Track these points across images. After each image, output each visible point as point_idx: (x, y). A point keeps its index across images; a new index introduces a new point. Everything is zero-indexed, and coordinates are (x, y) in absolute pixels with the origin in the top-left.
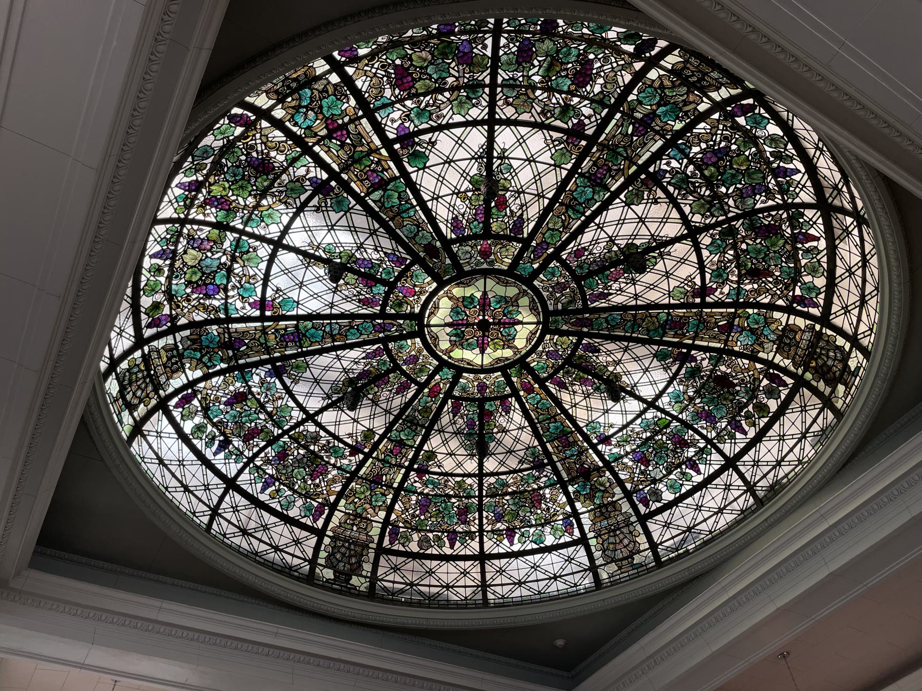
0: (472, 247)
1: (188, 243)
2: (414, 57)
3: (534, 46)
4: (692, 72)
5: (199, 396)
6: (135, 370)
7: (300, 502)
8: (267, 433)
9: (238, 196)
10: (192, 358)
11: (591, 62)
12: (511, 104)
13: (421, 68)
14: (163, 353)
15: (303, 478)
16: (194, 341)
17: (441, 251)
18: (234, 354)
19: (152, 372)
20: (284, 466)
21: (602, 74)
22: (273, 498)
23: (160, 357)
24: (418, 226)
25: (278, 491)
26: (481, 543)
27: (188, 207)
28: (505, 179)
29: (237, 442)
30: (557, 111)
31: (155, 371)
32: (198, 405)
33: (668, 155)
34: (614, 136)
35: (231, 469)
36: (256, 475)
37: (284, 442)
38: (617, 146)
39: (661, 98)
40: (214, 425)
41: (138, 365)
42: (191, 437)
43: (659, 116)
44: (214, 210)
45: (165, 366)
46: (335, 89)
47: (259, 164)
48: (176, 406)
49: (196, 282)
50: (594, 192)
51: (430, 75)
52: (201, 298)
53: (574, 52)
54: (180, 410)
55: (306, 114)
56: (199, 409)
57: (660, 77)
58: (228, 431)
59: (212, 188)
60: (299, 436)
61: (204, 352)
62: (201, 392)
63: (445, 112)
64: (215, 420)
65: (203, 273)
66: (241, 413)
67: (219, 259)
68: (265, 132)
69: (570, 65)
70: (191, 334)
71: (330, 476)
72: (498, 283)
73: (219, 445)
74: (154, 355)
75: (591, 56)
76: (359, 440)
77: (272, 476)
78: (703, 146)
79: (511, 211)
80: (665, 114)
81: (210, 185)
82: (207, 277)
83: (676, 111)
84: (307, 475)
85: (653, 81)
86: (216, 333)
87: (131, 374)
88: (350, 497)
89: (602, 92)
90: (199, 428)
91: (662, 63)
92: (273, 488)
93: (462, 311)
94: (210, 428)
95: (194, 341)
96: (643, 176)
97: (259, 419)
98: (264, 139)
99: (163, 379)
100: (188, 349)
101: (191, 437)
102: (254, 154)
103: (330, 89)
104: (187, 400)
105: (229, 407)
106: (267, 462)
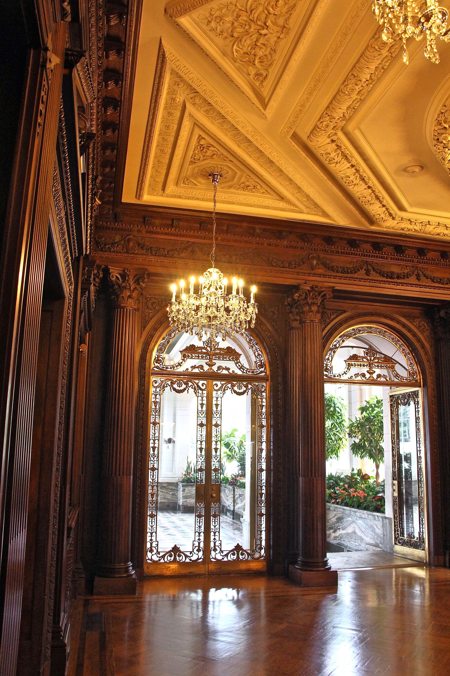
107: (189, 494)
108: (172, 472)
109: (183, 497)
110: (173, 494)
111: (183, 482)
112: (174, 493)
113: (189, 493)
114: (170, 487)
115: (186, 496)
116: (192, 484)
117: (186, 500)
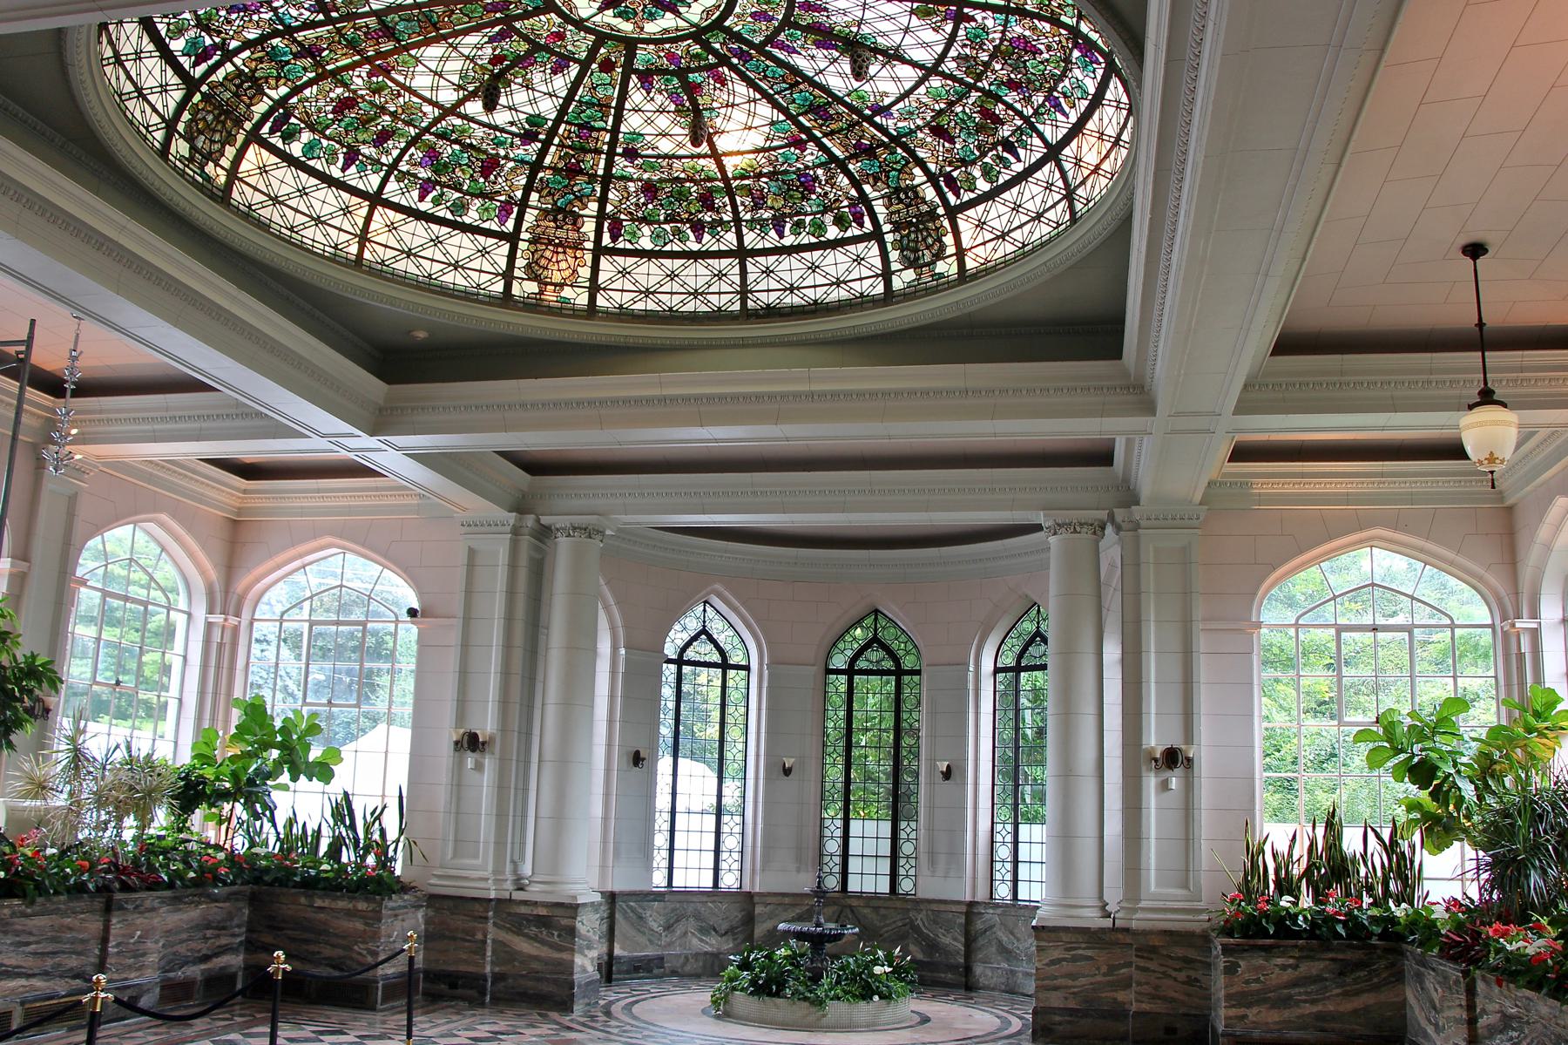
0: (565, 47)
1: (761, 208)
2: (468, 176)
3: (373, 140)
4: (246, 95)
5: (949, 169)
6: (905, 242)
7: (1077, 73)
8: (983, 101)
9: (690, 193)
10: (898, 179)
11: (333, 112)
12: (421, 111)
13: (470, 167)
14: (893, 209)
15: (1042, 63)
16: (877, 180)
17: (598, 60)
18: (878, 146)
19: (914, 220)
20: (1029, 83)
21: (328, 100)
22: (1075, 105)
23: (898, 212)
24: (594, 88)
25: (1064, 94)
26: (740, 237)
27: (721, 222)
28: (475, 72)
29: (1005, 131)
30: (386, 92)
31: (913, 217)
32: (958, 171)
33: (297, 20)
34: (343, 55)
35: (1035, 150)
36: (1046, 116)
37: (990, 85)
38: (346, 46)
39: (283, 67)
40: (984, 154)
41: (902, 237)
42: (995, 184)
43: (291, 53)
44: (717, 201)
45: (908, 206)
46: (542, 189)
47: (651, 192)
48: (958, 195)
49: (802, 193)
50: (396, 24)
51: (469, 158)
52: (820, 183)
53: (343, 124)
54: (962, 191)
55: (579, 191)
56: (963, 169)
57: (277, 88)
58: (991, 140)
59: (693, 211)
60: (972, 73)
61: (888, 169)
62: (942, 167)
63: (481, 134)
64: (978, 154)
65: (789, 190)
66: (962, 128)
67: (766, 183)
68: (617, 204)
69: (353, 115)
70: (869, 183)
71: (1027, 33)
72: (576, 7)
73: (1009, 152)
74: (895, 218)
75: (330, 116)
76: (939, 18)
77: (1047, 99)
78: (255, 17)
79: (494, 50)
80: (285, 54)
81: (691, 214)
82: (793, 185)
83: (273, 55)
84: (1035, 59)
85: (284, 84)
86: (859, 164)
87: (907, 249)
88: (1052, 10)
89: (336, 86)
90: (987, 173)
91: (271, 103)
92: (1062, 100)
93: (644, 13)
94: (987, 160)
95: (877, 180)
96: (334, 14)
97: (964, 112)
98: (624, 201)
99: (924, 208)
100: (887, 184)
101: (995, 184)
102: (642, 200)
103: (545, 192)
104: (952, 183)
105: (956, 140)
106: (1028, 100)
107: (1255, 986)
108: (1186, 887)
109: (1228, 997)
110: (1191, 981)
111: (1227, 930)
112: (1193, 974)
113: (1257, 980)
114: (1179, 952)
115: (1243, 994)
116: (1268, 941)
117: (1241, 1011)
